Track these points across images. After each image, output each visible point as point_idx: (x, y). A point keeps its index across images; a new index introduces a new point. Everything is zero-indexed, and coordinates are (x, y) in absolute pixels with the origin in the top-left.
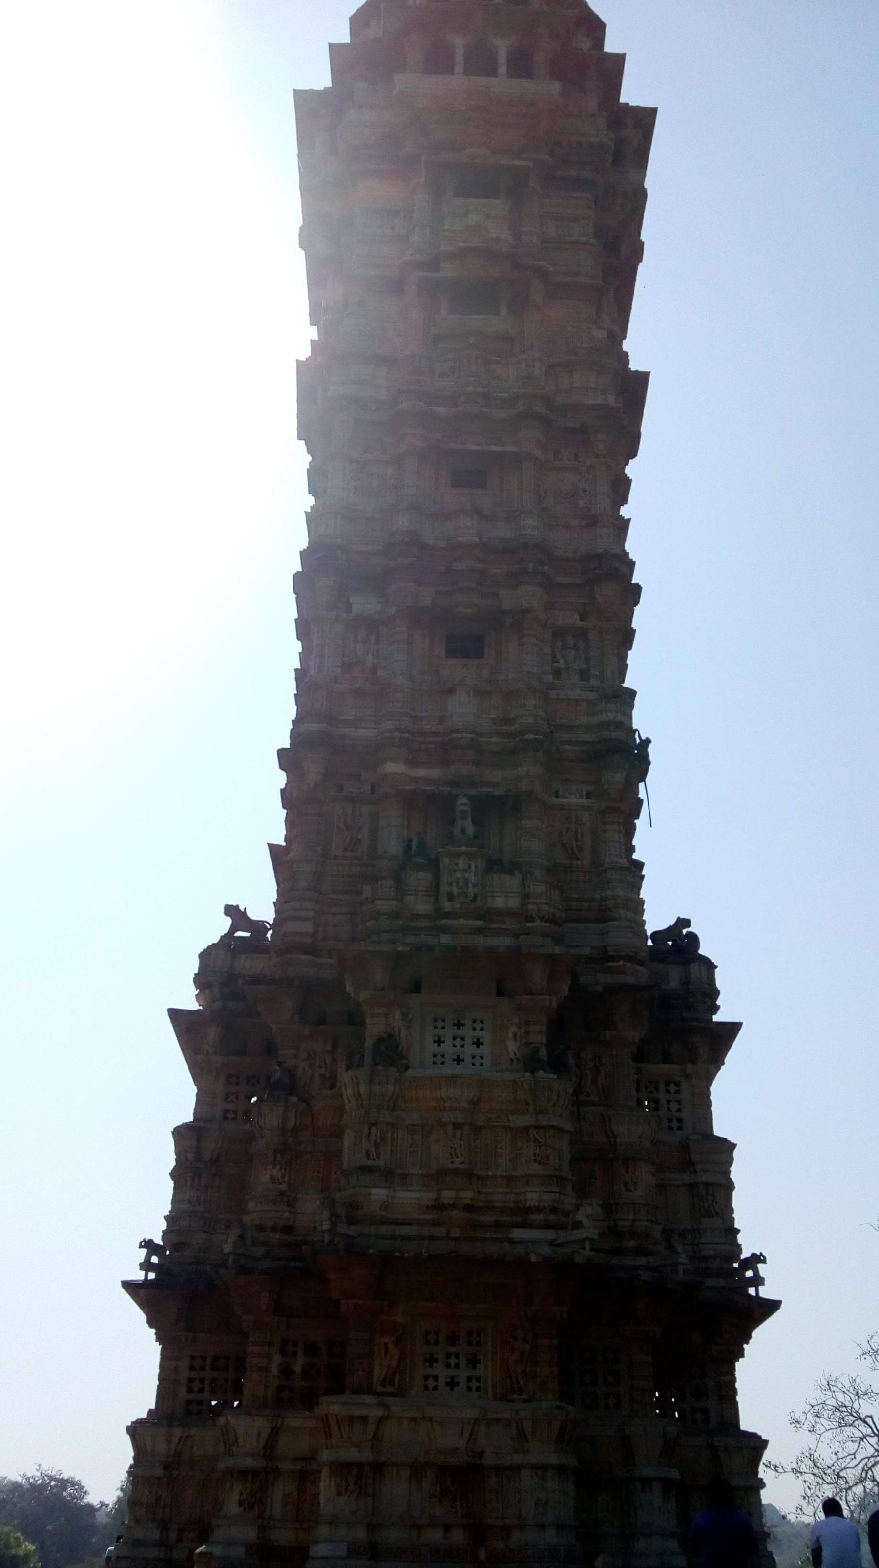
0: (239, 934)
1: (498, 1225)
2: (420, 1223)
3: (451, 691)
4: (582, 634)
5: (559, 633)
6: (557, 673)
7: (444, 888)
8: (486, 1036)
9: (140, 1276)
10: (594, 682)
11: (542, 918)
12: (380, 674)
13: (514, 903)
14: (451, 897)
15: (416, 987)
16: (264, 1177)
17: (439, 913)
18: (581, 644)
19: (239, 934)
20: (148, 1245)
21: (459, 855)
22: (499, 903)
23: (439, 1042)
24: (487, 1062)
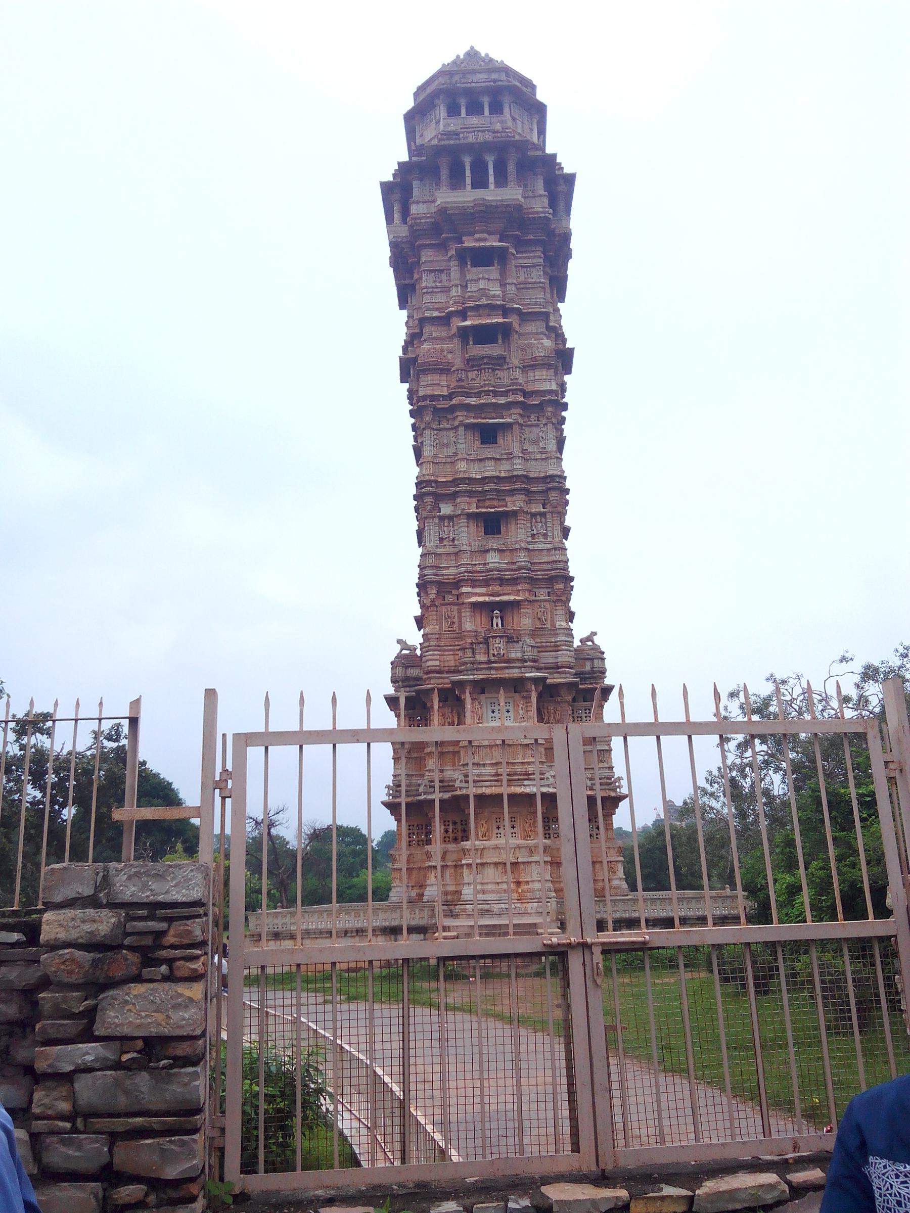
0: (404, 652)
1: (519, 780)
2: (491, 781)
3: (488, 551)
4: (543, 515)
5: (533, 515)
6: (533, 536)
7: (491, 652)
8: (511, 710)
9: (386, 798)
10: (549, 539)
11: (530, 661)
12: (456, 542)
13: (519, 655)
14: (494, 655)
15: (483, 692)
16: (431, 763)
17: (489, 662)
18: (543, 520)
19: (404, 652)
20: (388, 787)
21: (496, 637)
22: (513, 655)
23: (493, 712)
24: (512, 718)
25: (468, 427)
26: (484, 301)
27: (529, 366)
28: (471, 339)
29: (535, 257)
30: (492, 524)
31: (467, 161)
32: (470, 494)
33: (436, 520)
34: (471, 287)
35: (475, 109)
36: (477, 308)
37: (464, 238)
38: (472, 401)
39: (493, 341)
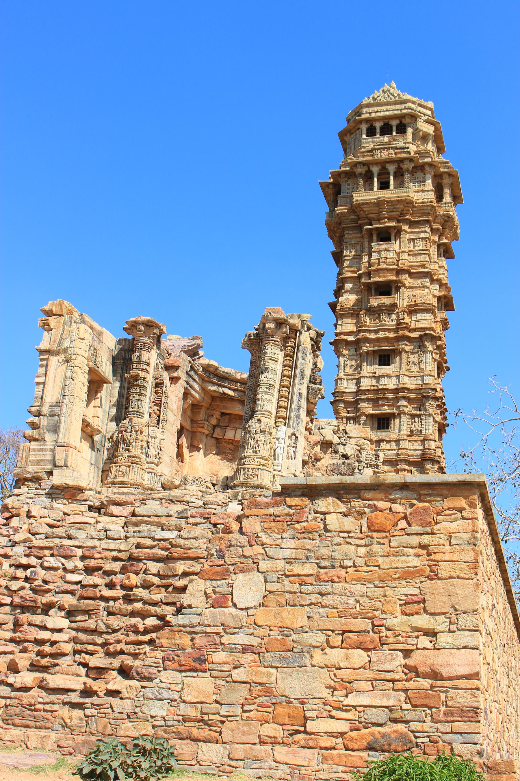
4: (419, 416)
5: (413, 416)
25: (367, 353)
26: (383, 266)
27: (414, 310)
28: (373, 291)
29: (422, 232)
30: (383, 422)
31: (375, 170)
32: (368, 400)
33: (344, 420)
34: (375, 256)
35: (386, 130)
36: (378, 270)
37: (373, 222)
38: (372, 336)
39: (388, 293)
